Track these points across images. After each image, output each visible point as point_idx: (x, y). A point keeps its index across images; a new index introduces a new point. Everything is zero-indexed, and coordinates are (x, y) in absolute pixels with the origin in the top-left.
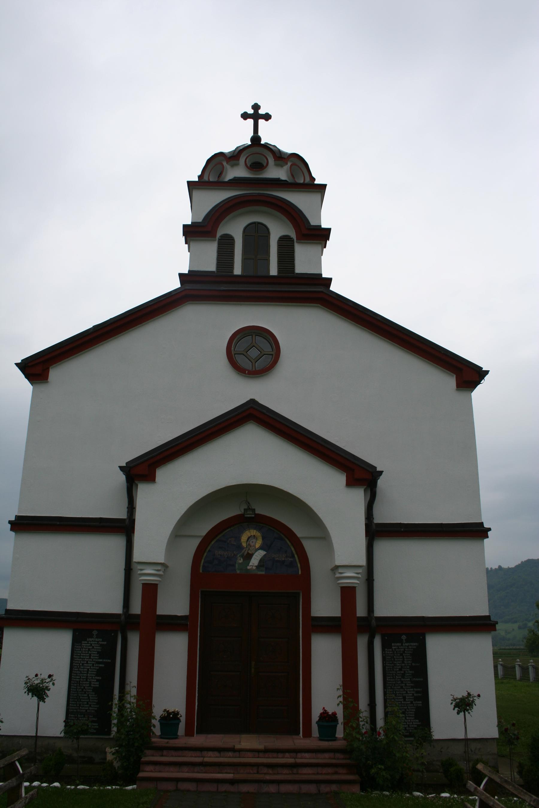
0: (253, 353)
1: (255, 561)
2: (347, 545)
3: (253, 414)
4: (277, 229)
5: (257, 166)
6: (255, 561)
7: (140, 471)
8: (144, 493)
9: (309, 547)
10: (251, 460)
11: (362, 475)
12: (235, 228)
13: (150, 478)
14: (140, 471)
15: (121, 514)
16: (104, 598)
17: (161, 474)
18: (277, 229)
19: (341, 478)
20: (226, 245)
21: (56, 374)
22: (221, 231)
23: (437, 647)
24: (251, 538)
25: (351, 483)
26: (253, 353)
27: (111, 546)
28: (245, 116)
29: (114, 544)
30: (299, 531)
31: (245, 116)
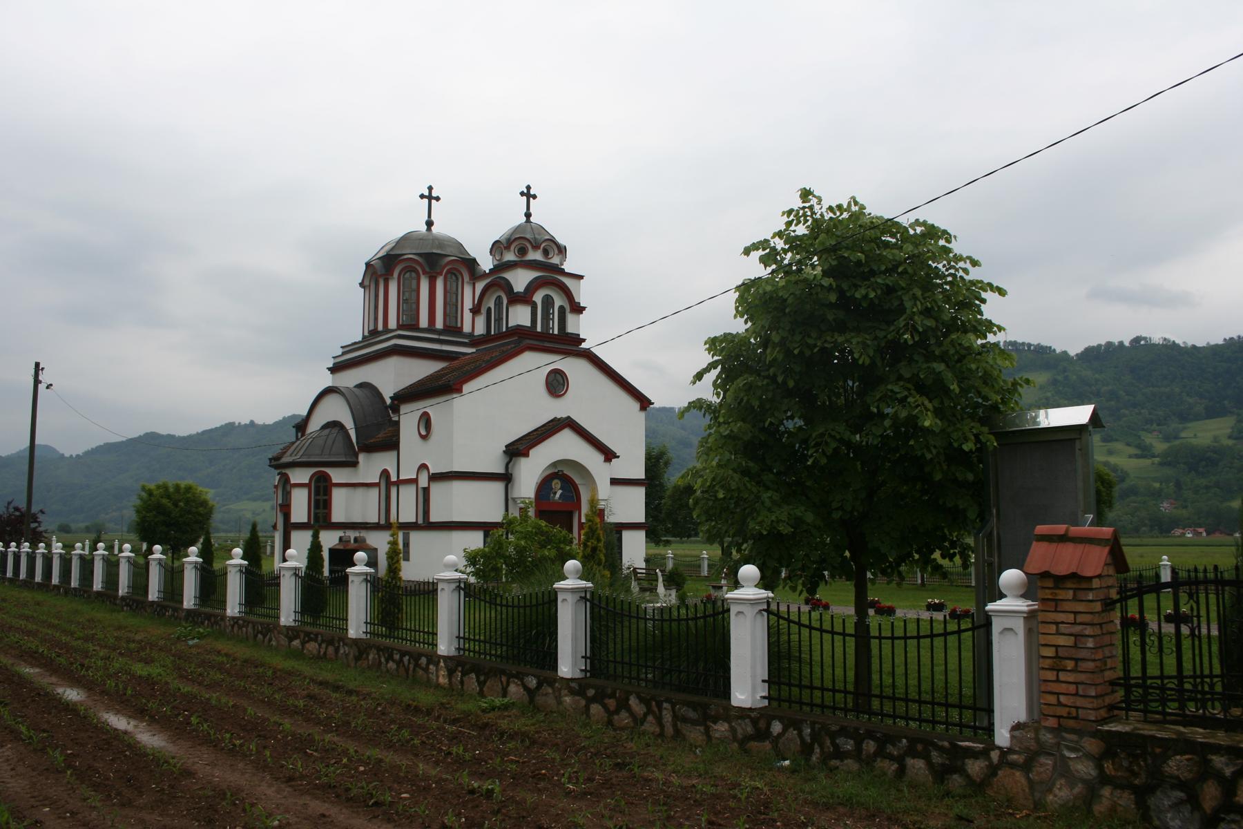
0: (556, 384)
1: (558, 496)
2: (604, 490)
3: (569, 424)
4: (559, 301)
5: (546, 253)
6: (558, 496)
7: (517, 450)
9: (582, 490)
10: (564, 446)
11: (609, 455)
18: (559, 301)
20: (534, 307)
23: (627, 536)
24: (556, 484)
26: (556, 384)
29: (498, 487)
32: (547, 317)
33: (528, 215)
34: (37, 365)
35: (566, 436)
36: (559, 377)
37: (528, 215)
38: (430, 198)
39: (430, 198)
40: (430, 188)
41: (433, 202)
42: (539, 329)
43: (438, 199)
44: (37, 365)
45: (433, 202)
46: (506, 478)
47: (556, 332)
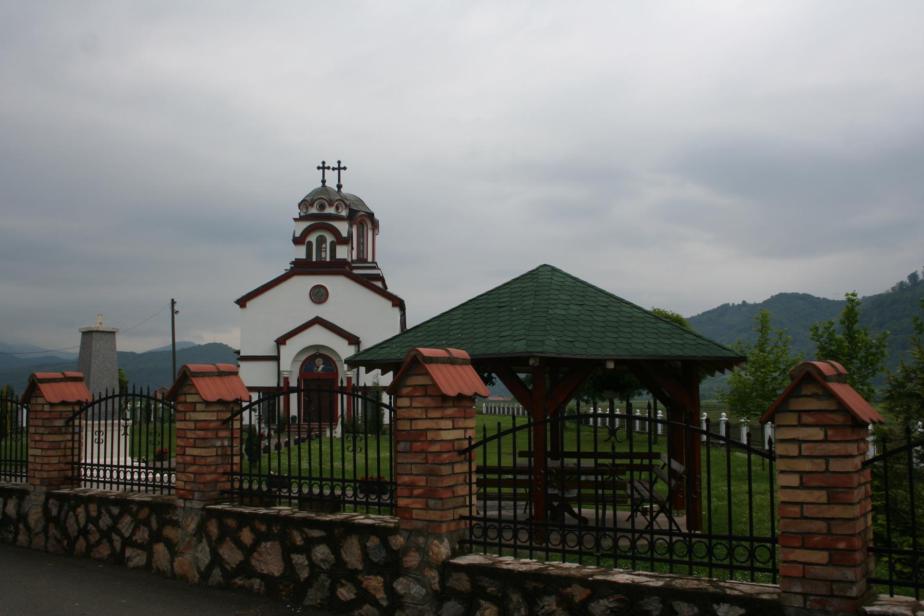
0: (319, 295)
1: (320, 369)
3: (318, 321)
4: (330, 238)
6: (320, 369)
7: (281, 341)
8: (282, 348)
10: (318, 336)
12: (313, 238)
13: (284, 344)
14: (281, 341)
15: (275, 354)
16: (273, 383)
17: (288, 342)
19: (346, 342)
20: (310, 245)
21: (248, 304)
22: (307, 240)
25: (350, 344)
26: (319, 295)
27: (272, 365)
28: (319, 168)
30: (334, 359)
31: (319, 168)
32: (319, 250)
33: (324, 182)
34: (173, 300)
35: (317, 328)
36: (322, 290)
37: (324, 182)
38: (339, 169)
39: (339, 169)
40: (339, 162)
41: (342, 171)
42: (314, 259)
43: (345, 168)
44: (173, 300)
45: (342, 171)
46: (276, 358)
47: (328, 259)
